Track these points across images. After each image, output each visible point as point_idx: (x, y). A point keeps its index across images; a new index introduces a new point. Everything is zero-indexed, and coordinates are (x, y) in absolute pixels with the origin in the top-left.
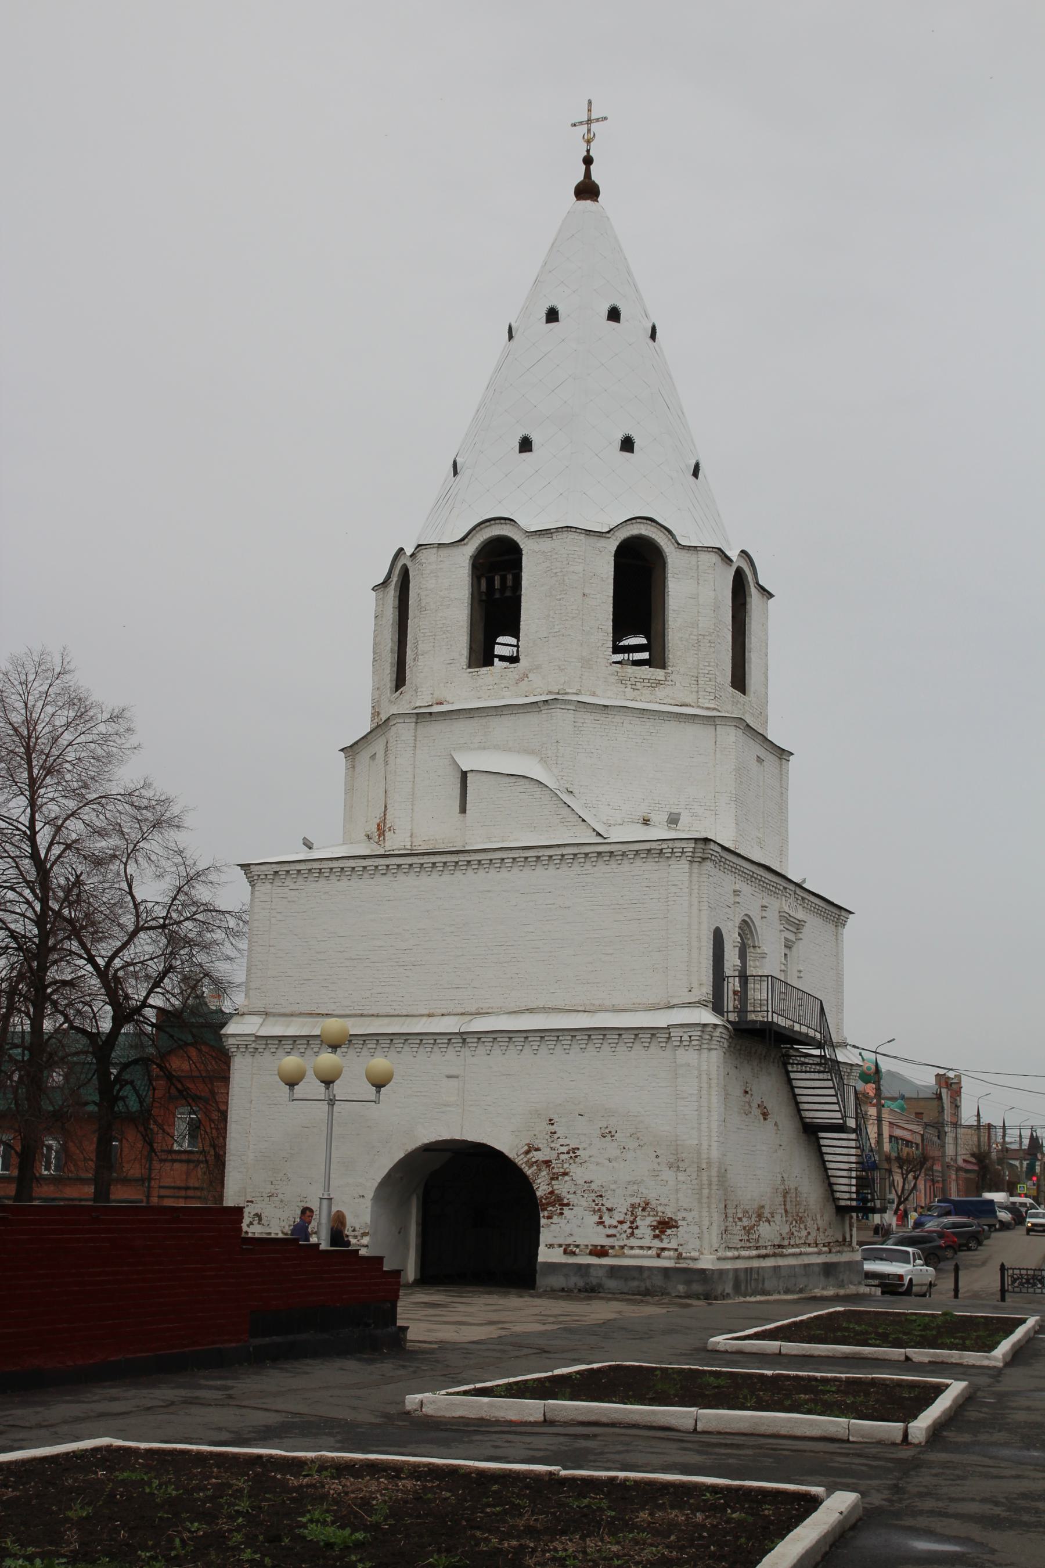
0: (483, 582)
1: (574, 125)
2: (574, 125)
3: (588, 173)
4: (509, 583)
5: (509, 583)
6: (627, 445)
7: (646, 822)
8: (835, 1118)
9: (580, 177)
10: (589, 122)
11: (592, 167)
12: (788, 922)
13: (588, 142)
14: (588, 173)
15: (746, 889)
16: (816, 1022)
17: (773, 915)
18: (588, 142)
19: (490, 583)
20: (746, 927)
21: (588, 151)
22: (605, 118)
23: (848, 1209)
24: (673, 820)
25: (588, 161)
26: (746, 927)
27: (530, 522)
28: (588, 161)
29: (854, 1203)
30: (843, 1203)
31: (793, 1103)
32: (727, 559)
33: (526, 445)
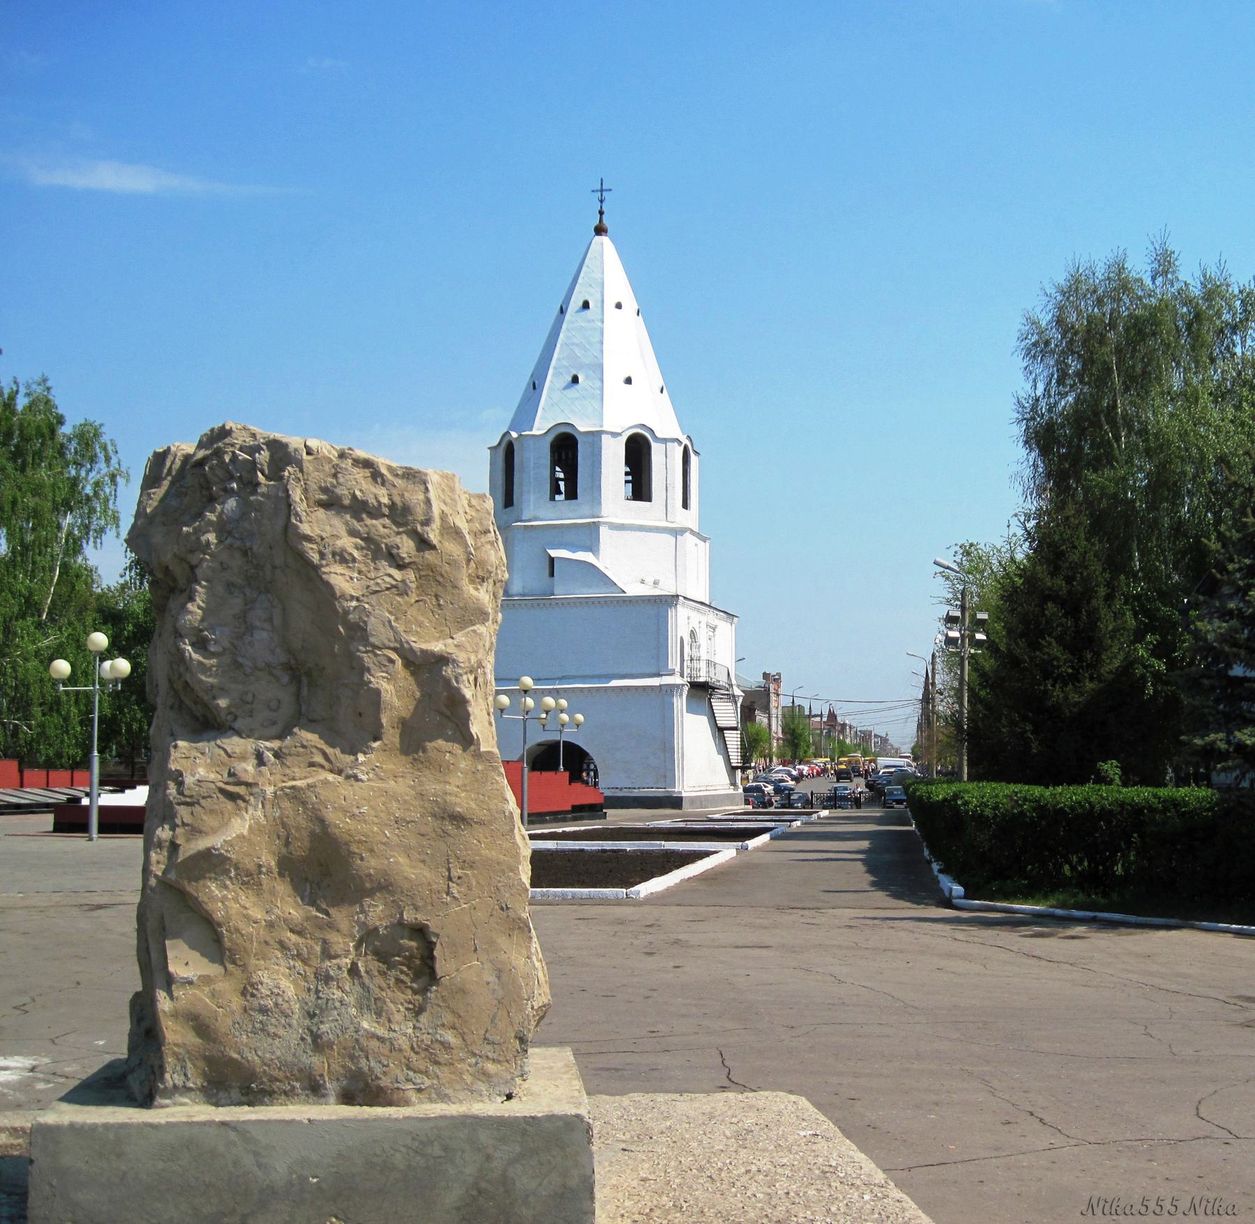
0: (556, 454)
1: (593, 191)
2: (593, 191)
3: (601, 220)
4: (570, 455)
5: (570, 455)
6: (628, 381)
7: (643, 582)
8: (734, 724)
9: (597, 222)
10: (602, 191)
11: (604, 216)
12: (710, 627)
13: (601, 201)
14: (601, 220)
15: (693, 614)
16: (726, 680)
17: (703, 625)
18: (601, 201)
19: (560, 456)
20: (693, 634)
21: (601, 207)
22: (610, 190)
23: (737, 768)
24: (656, 583)
25: (601, 213)
26: (693, 634)
27: (581, 429)
28: (601, 213)
29: (739, 765)
30: (734, 765)
31: (713, 720)
32: (680, 442)
33: (575, 380)
